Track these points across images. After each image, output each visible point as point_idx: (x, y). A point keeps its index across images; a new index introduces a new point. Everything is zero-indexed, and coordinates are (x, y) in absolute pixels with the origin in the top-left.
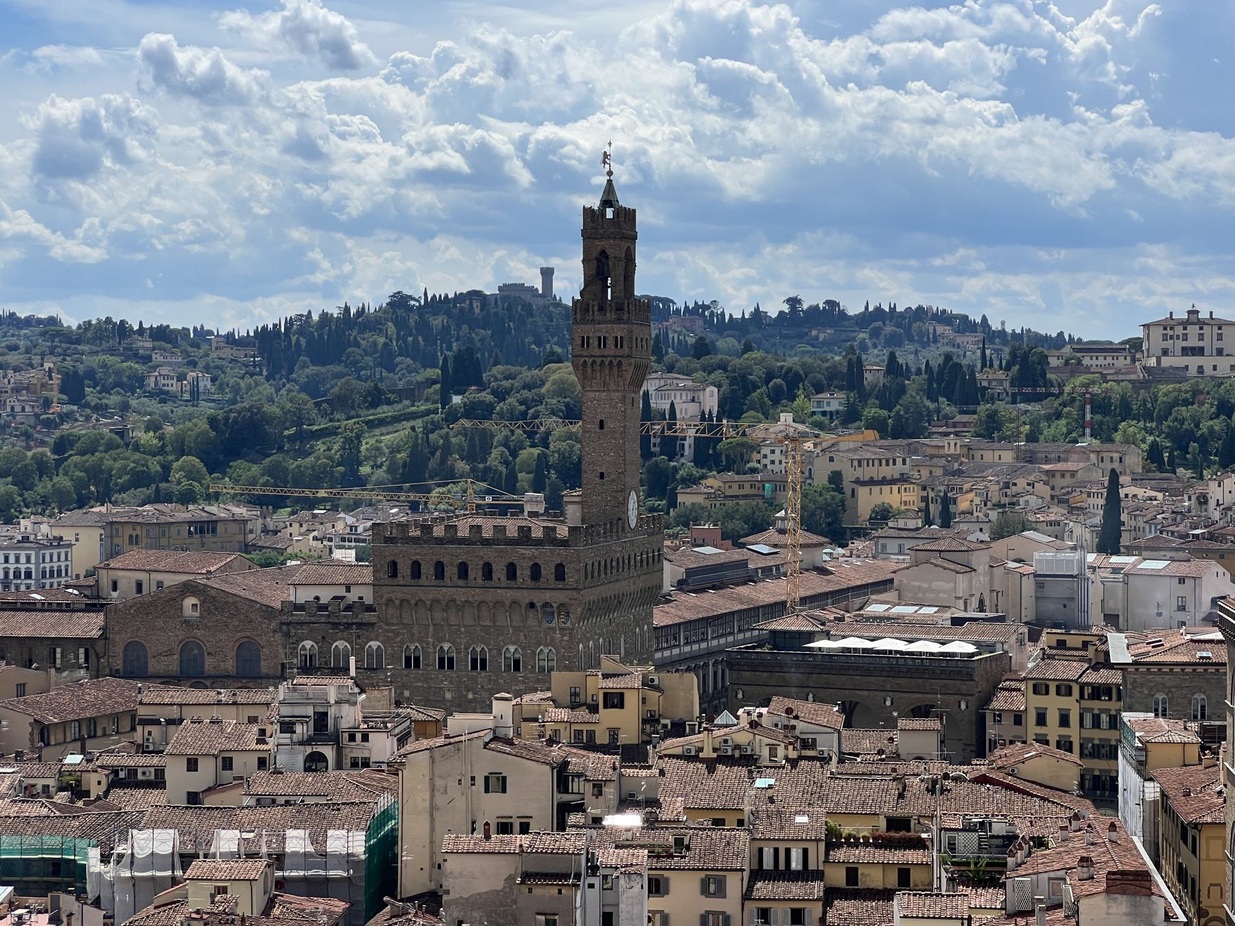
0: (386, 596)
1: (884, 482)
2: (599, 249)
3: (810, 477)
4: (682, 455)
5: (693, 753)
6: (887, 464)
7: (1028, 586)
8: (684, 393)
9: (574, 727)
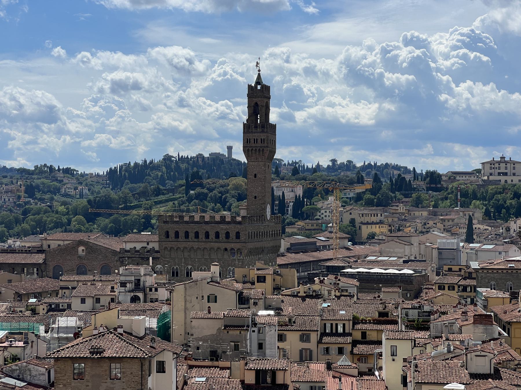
1: (373, 223)
3: (342, 221)
4: (287, 214)
5: (296, 294)
6: (374, 216)
7: (435, 253)
8: (288, 188)
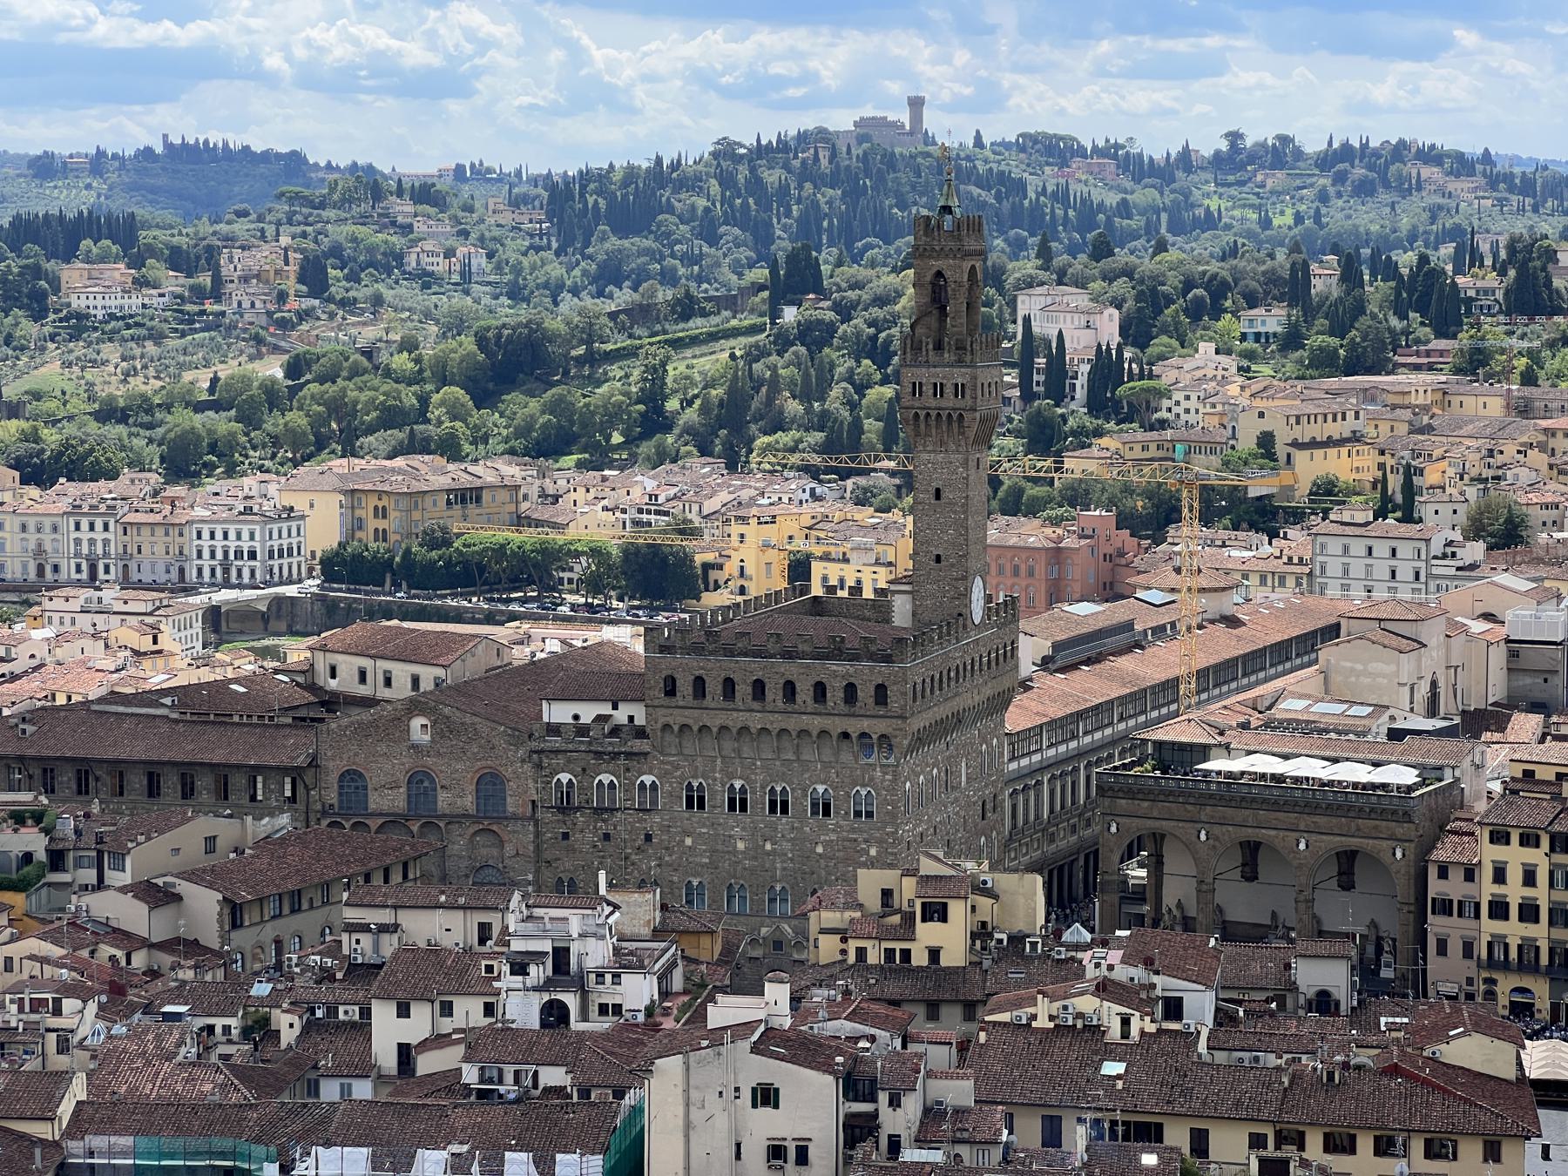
0: (662, 721)
1: (1329, 443)
2: (934, 270)
3: (1234, 437)
4: (1073, 398)
5: (1024, 1021)
6: (1335, 420)
7: (1498, 656)
8: (1076, 316)
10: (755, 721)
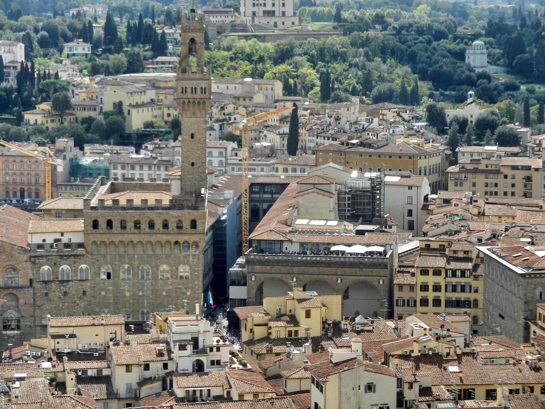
0: (92, 240)
2: (191, 37)
3: (102, 103)
5: (408, 354)
9: (288, 329)
10: (136, 238)
